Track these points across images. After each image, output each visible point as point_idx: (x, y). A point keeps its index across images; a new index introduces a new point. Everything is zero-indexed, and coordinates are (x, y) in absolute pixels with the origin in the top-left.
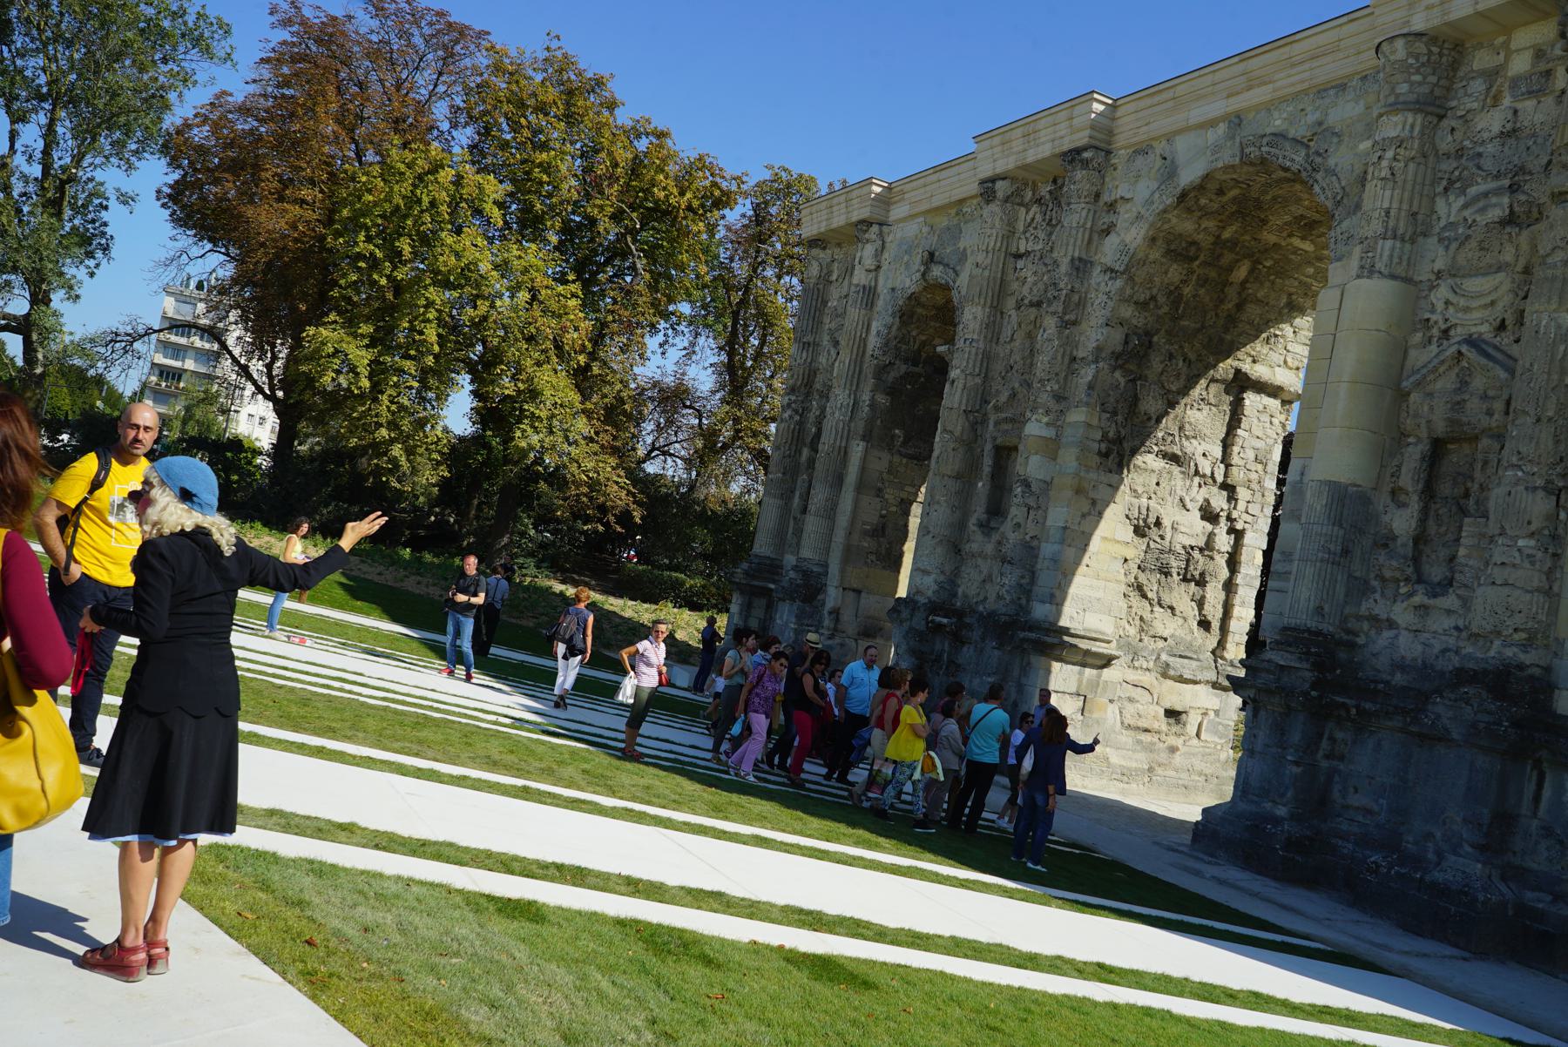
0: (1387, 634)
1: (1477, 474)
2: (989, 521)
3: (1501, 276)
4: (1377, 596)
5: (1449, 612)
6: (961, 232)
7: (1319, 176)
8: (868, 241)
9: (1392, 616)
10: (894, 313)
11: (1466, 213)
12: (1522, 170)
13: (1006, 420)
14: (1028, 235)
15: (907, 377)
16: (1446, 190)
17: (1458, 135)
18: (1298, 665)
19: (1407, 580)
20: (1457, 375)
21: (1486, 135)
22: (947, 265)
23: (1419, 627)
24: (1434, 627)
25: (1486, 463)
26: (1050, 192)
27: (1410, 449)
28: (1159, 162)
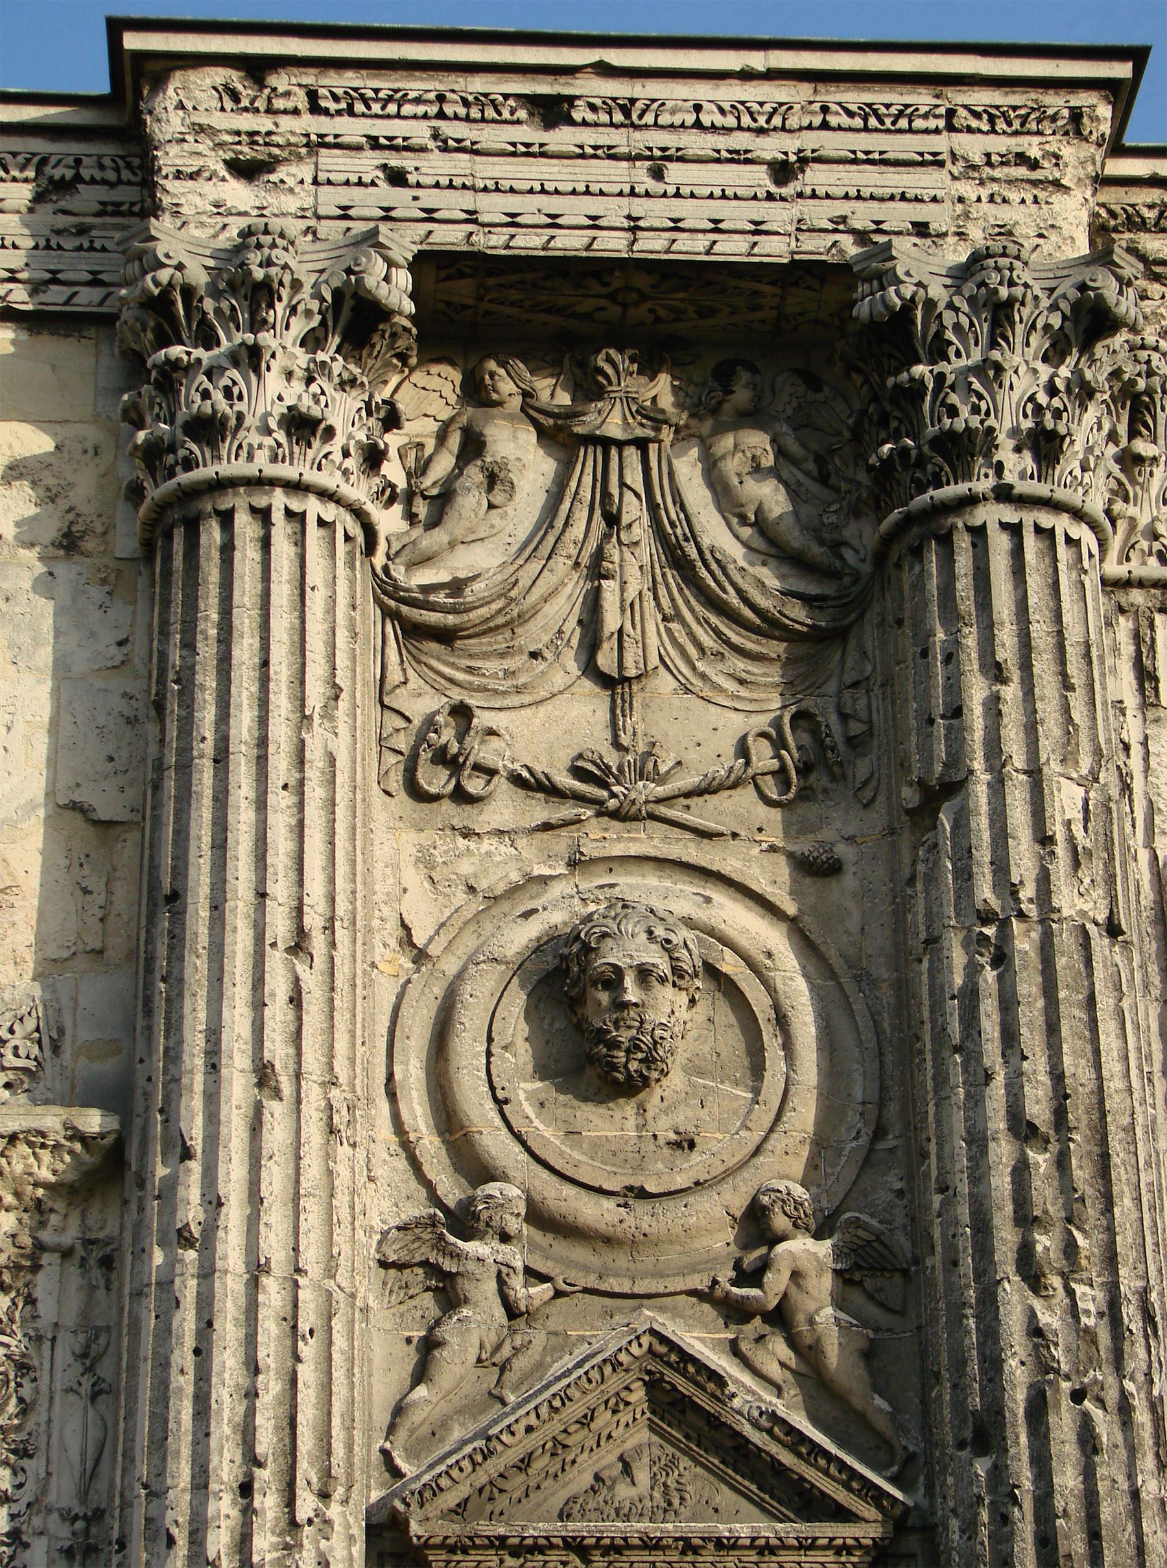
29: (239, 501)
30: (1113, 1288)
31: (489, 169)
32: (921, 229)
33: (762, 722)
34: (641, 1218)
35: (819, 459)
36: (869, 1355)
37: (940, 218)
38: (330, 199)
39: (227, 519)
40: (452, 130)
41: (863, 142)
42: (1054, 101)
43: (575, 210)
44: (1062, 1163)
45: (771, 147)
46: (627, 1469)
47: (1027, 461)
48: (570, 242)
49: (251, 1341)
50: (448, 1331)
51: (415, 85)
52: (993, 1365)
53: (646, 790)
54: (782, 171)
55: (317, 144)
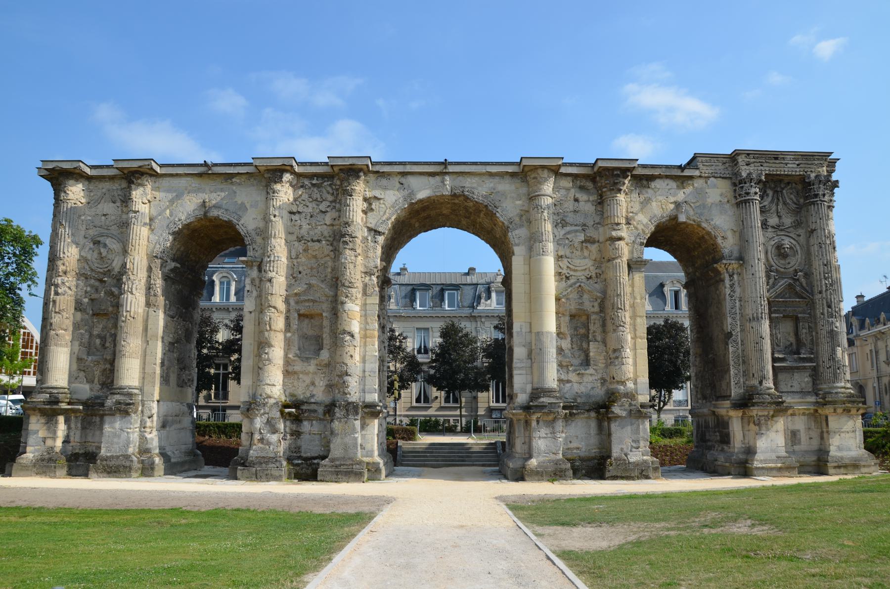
0: (568, 385)
1: (592, 327)
2: (300, 354)
3: (587, 260)
4: (562, 372)
5: (591, 375)
6: (235, 192)
7: (498, 210)
8: (142, 185)
9: (569, 378)
10: (174, 233)
11: (568, 236)
12: (585, 225)
13: (305, 301)
14: (298, 203)
15: (173, 270)
16: (556, 226)
17: (558, 208)
18: (557, 401)
19: (572, 365)
20: (578, 293)
21: (568, 210)
22: (226, 210)
23: (581, 381)
24: (587, 380)
25: (594, 323)
26: (314, 185)
27: (562, 318)
28: (398, 185)
29: (751, 201)
30: (832, 279)
31: (770, 165)
32: (811, 171)
33: (793, 220)
34: (786, 270)
35: (797, 192)
36: (806, 283)
37: (813, 170)
38: (756, 168)
39: (749, 203)
40: (767, 161)
41: (805, 162)
42: (824, 158)
43: (779, 169)
44: (827, 267)
45: (797, 162)
46: (786, 294)
47: (822, 197)
48: (778, 173)
49: (760, 284)
50: (770, 281)
51: (764, 156)
52: (821, 286)
53: (783, 227)
54: (798, 165)
55: (754, 162)
